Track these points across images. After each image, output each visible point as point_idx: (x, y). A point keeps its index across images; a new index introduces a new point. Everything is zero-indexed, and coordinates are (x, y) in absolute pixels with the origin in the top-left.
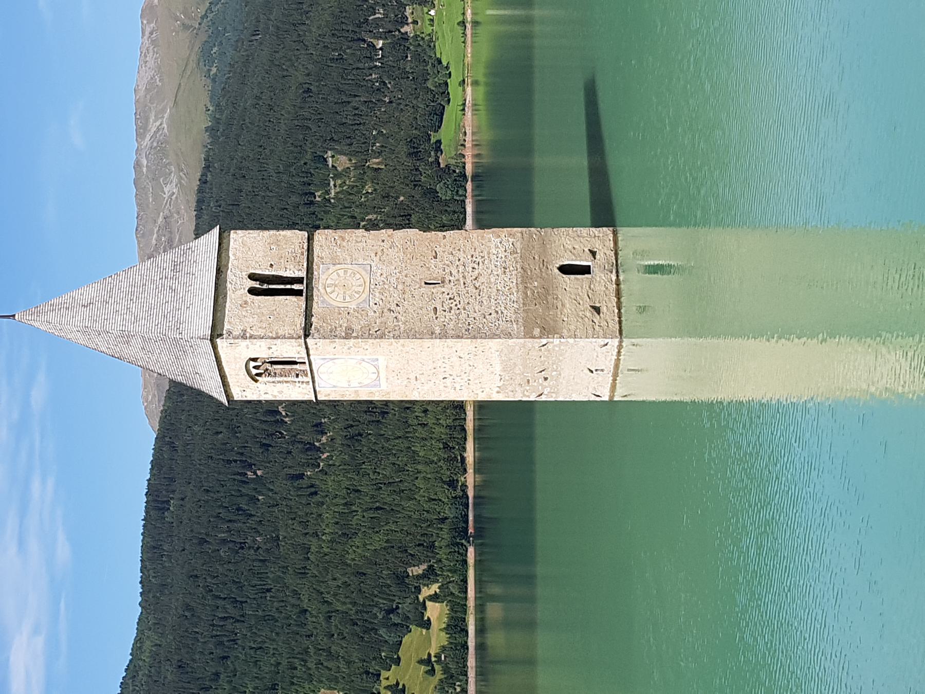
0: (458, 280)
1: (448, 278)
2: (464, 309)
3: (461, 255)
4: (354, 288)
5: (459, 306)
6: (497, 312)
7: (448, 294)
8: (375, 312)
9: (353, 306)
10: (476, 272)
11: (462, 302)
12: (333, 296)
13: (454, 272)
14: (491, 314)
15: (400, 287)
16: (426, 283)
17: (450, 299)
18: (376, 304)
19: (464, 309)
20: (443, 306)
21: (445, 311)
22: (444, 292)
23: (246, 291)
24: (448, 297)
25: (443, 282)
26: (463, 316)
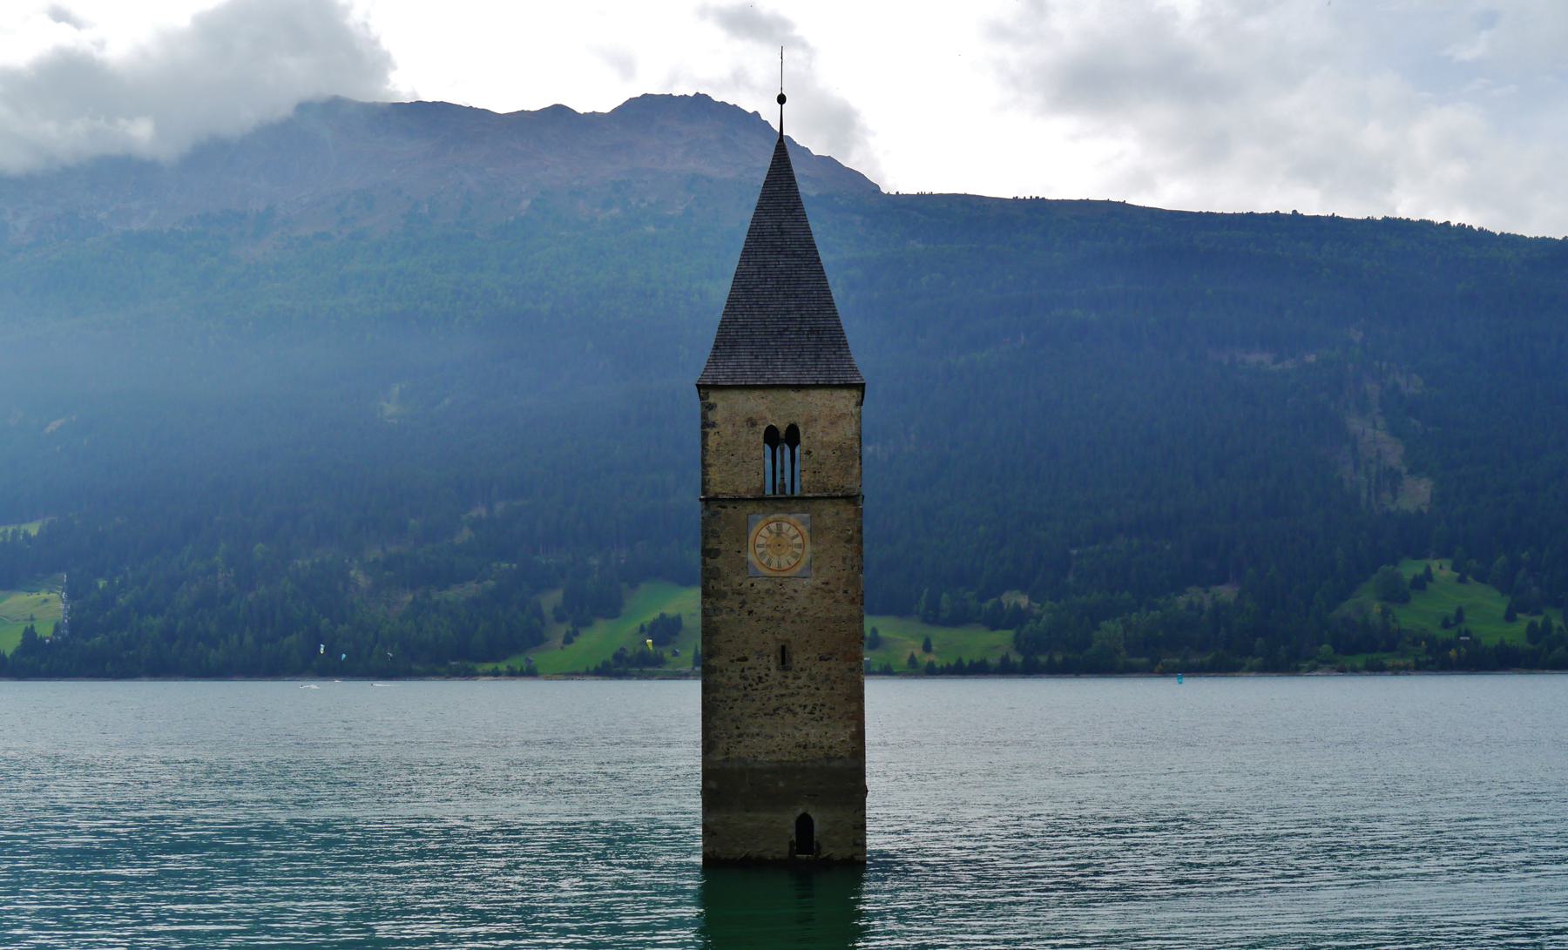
0: (787, 687)
1: (790, 675)
2: (746, 695)
3: (822, 692)
4: (776, 557)
5: (749, 688)
6: (740, 735)
7: (767, 675)
8: (740, 585)
9: (751, 557)
10: (798, 710)
11: (755, 692)
12: (764, 532)
13: (799, 682)
14: (738, 728)
15: (778, 615)
16: (783, 648)
17: (760, 678)
18: (752, 585)
19: (746, 695)
20: (750, 668)
21: (743, 671)
22: (769, 670)
23: (770, 423)
24: (762, 675)
25: (786, 669)
26: (735, 694)
